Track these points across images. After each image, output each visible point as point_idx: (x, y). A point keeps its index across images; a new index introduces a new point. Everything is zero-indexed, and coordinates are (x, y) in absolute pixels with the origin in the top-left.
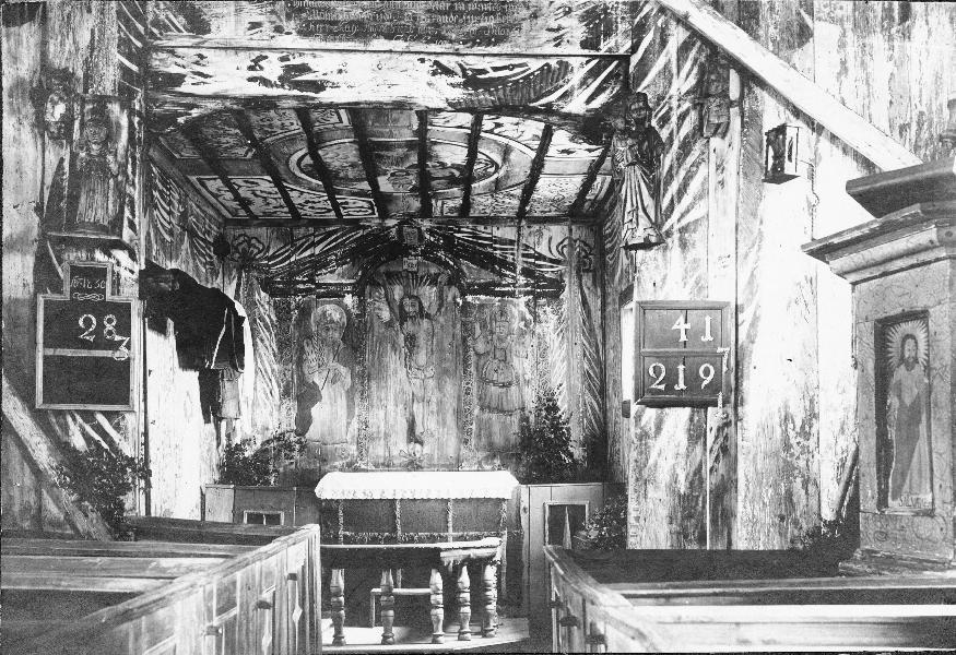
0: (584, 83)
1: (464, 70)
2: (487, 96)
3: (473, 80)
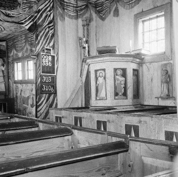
3: (8, 16)
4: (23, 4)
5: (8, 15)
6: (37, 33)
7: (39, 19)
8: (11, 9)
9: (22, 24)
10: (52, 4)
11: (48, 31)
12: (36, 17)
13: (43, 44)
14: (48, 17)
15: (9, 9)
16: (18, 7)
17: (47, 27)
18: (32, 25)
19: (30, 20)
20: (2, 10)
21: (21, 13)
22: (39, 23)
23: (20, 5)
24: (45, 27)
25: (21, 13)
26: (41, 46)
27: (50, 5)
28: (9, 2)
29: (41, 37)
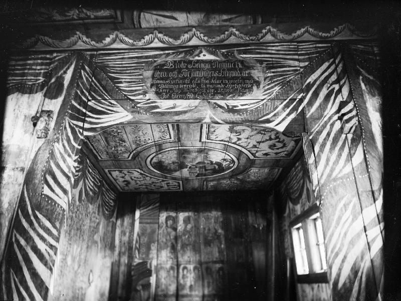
0: (284, 109)
1: (228, 106)
2: (239, 116)
3: (232, 110)
4: (265, 80)
5: (232, 109)
6: (311, 138)
7: (310, 104)
8: (239, 96)
9: (268, 121)
10: (341, 65)
11: (342, 128)
12: (301, 100)
13: (331, 163)
14: (334, 95)
15: (234, 96)
16: (255, 88)
17: (336, 117)
18: (294, 121)
19: (288, 111)
20: (219, 102)
21: (263, 100)
22: (312, 114)
23: (259, 84)
24: (330, 118)
25: (263, 100)
26: (325, 167)
27: (335, 69)
28: (232, 84)
29: (323, 146)
